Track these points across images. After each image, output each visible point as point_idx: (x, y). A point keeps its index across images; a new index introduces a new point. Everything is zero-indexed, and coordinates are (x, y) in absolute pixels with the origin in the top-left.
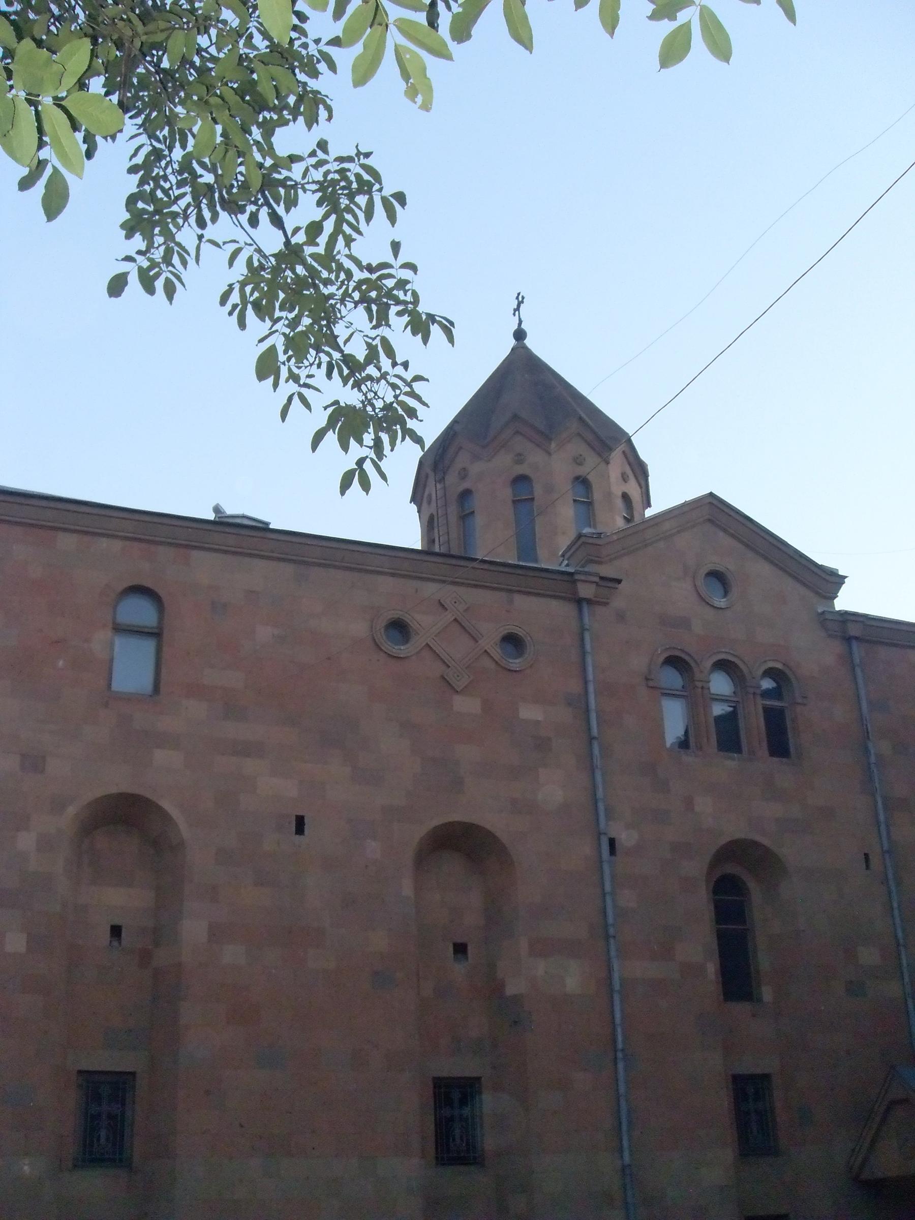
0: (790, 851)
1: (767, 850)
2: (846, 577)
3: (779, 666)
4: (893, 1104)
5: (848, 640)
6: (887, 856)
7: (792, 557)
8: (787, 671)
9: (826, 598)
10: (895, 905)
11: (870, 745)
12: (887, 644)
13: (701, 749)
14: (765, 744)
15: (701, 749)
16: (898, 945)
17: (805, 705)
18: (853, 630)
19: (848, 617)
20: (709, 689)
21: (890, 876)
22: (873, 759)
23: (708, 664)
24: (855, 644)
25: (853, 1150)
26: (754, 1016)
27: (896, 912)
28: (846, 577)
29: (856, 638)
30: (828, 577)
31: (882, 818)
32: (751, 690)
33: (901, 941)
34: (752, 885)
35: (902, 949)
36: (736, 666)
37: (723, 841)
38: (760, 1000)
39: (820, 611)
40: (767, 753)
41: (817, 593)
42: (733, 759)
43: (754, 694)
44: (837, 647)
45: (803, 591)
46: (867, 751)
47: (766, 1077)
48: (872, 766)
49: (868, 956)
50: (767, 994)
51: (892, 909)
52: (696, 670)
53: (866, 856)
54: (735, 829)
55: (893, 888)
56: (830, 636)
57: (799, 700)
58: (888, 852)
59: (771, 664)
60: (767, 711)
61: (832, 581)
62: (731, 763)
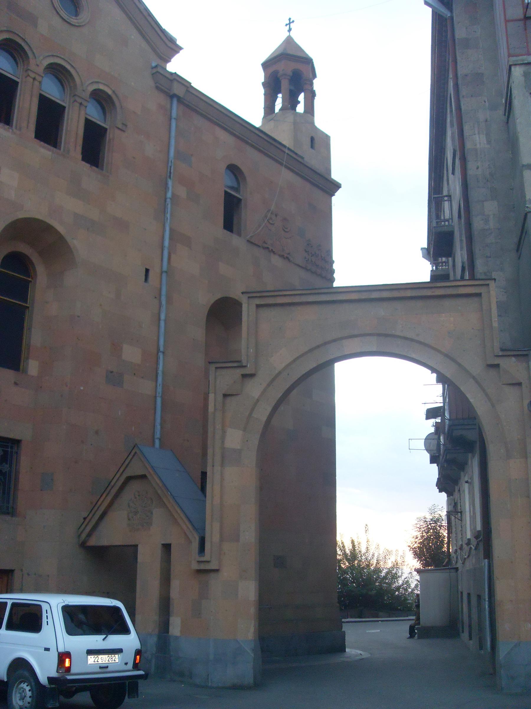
0: (79, 243)
1: (61, 238)
2: (181, 48)
3: (110, 92)
4: (129, 479)
5: (172, 96)
6: (164, 275)
7: (141, 12)
8: (114, 97)
9: (161, 58)
10: (163, 317)
11: (170, 183)
12: (202, 115)
13: (20, 129)
14: (79, 149)
15: (20, 129)
16: (158, 350)
17: (124, 131)
18: (177, 90)
19: (176, 78)
20: (40, 82)
21: (164, 292)
22: (169, 195)
23: (46, 63)
24: (175, 101)
25: (85, 519)
26: (16, 384)
27: (162, 324)
28: (181, 48)
29: (179, 99)
30: (167, 41)
31: (167, 243)
32: (80, 100)
33: (162, 349)
34: (40, 270)
35: (161, 356)
36: (71, 75)
37: (21, 215)
38: (25, 371)
39: (154, 65)
40: (80, 157)
41: (154, 50)
42: (49, 150)
43: (81, 104)
44: (162, 99)
45: (144, 45)
46: (166, 187)
47: (17, 442)
48: (168, 200)
49: (131, 354)
50: (33, 367)
51: (159, 319)
52: (32, 61)
53: (147, 271)
54: (34, 208)
55: (164, 302)
56: (157, 88)
57: (120, 126)
58: (166, 272)
59: (101, 87)
60: (89, 124)
61: (168, 46)
62: (44, 151)
